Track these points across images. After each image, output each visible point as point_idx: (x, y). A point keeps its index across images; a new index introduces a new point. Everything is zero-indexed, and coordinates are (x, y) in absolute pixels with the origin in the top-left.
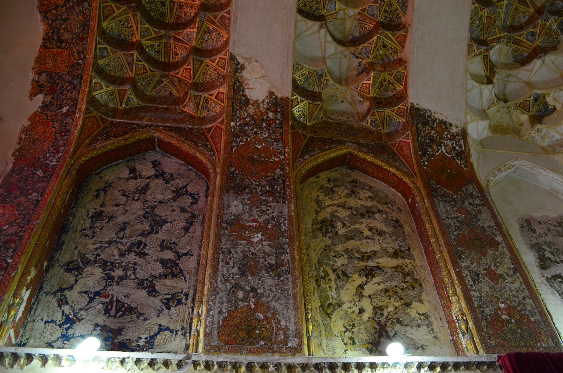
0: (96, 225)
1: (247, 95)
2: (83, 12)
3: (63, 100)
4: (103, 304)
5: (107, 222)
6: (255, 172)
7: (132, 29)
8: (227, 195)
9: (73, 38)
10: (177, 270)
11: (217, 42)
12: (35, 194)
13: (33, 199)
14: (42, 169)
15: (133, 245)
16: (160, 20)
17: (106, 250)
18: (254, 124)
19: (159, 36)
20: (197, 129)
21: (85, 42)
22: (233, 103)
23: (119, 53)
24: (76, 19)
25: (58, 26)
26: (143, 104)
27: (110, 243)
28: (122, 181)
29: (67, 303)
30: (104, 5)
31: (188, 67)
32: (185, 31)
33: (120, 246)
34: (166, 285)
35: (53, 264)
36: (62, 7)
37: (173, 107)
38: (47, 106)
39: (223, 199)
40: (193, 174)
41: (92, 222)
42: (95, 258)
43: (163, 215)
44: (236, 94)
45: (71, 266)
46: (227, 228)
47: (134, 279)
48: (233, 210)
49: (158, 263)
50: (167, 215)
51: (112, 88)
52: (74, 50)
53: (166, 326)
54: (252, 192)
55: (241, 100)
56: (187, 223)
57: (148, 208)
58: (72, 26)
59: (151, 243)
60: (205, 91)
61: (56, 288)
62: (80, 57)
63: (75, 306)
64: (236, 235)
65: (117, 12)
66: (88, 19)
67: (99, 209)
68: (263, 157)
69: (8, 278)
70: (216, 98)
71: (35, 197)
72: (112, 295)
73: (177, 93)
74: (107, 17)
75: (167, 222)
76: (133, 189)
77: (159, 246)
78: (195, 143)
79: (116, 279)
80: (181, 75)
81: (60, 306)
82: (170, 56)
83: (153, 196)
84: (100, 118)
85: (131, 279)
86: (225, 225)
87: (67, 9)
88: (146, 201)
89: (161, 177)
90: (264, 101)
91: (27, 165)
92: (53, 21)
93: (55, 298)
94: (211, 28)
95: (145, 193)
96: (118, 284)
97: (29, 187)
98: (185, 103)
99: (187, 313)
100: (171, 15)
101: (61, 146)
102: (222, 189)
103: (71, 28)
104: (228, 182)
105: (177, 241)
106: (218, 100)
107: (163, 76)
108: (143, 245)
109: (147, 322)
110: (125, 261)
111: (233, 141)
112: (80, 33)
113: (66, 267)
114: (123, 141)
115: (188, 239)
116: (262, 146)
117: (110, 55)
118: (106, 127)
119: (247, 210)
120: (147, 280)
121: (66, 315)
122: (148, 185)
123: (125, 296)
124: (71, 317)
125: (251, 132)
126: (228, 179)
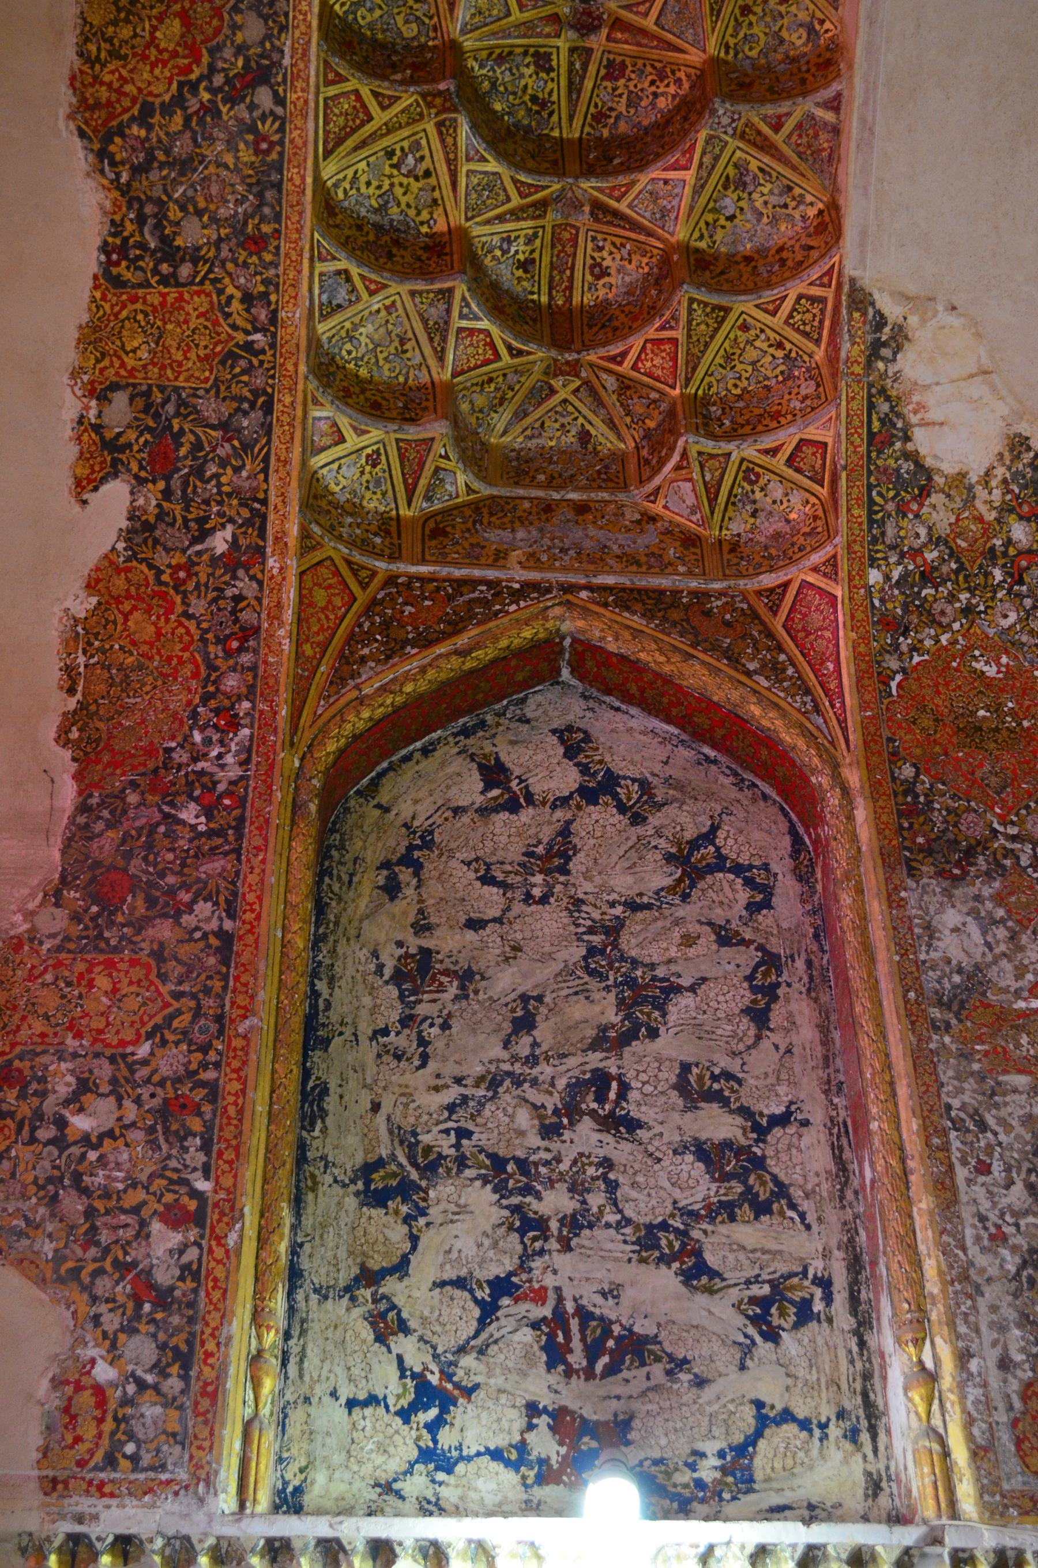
0: (422, 1010)
1: (922, 451)
2: (252, 129)
3: (207, 502)
4: (535, 1326)
5: (457, 998)
6: (994, 780)
7: (433, 181)
8: (910, 883)
9: (220, 240)
10: (764, 1183)
11: (774, 221)
12: (204, 908)
13: (207, 927)
14: (196, 800)
15: (576, 1087)
16: (528, 130)
17: (487, 1113)
18: (957, 572)
19: (534, 205)
20: (722, 594)
21: (268, 257)
22: (870, 487)
23: (394, 288)
24: (229, 159)
25: (157, 192)
26: (486, 491)
27: (494, 1082)
28: (466, 819)
29: (403, 1328)
30: (332, 91)
31: (666, 334)
32: (643, 179)
33: (533, 1095)
34: (744, 1248)
35: (313, 1176)
36: (167, 110)
37: (605, 495)
38: (149, 527)
39: (902, 904)
40: (727, 781)
41: (402, 997)
42: (457, 1146)
43: (656, 959)
44: (880, 452)
45: (378, 1184)
46: (948, 1027)
47: (618, 1226)
48: (949, 946)
49: (689, 1158)
50: (670, 961)
51: (376, 434)
52: (230, 290)
53: (779, 1407)
54: (1003, 867)
55: (899, 476)
56: (754, 989)
57: (591, 931)
58: (214, 190)
59: (643, 1077)
60: (743, 437)
61: (347, 1272)
62: (254, 321)
63: (435, 1339)
64: (986, 1054)
65: (380, 117)
66: (274, 156)
67: (414, 943)
68: (1013, 713)
69: (219, 1253)
70: (790, 462)
71: (208, 920)
72: (558, 1289)
73: (612, 437)
74: (340, 141)
75: (678, 989)
76: (515, 853)
77: (674, 1087)
78: (734, 661)
79: (554, 1225)
80: (635, 367)
81: (381, 1338)
82: (571, 279)
83: (598, 880)
84: (349, 563)
85: (608, 1225)
86: (935, 1013)
87: (187, 120)
88: (578, 902)
89: (608, 798)
90: (987, 474)
91: (133, 784)
92: (137, 170)
93: (357, 1312)
94: (754, 165)
95: (564, 871)
96: (566, 1247)
97: (171, 879)
98: (657, 481)
99: (842, 1353)
100: (573, 104)
101: (239, 699)
102: (887, 859)
103: (209, 199)
104: (901, 828)
105: (734, 1066)
106: (798, 470)
107: (554, 370)
108: (614, 1085)
109: (708, 1393)
110: (569, 1155)
111: (883, 651)
112: (247, 216)
113: (360, 1185)
114: (455, 662)
115: (777, 1056)
116: (998, 664)
117: (359, 299)
118: (374, 602)
119: (1003, 947)
120: (664, 1226)
121: (414, 1376)
122: (565, 832)
123: (604, 1295)
124: (434, 1379)
125: (949, 609)
126: (901, 814)
